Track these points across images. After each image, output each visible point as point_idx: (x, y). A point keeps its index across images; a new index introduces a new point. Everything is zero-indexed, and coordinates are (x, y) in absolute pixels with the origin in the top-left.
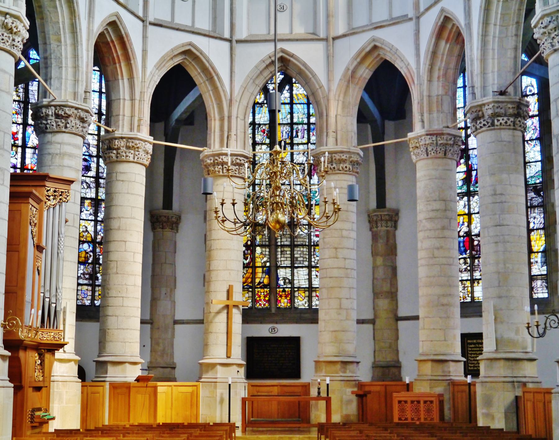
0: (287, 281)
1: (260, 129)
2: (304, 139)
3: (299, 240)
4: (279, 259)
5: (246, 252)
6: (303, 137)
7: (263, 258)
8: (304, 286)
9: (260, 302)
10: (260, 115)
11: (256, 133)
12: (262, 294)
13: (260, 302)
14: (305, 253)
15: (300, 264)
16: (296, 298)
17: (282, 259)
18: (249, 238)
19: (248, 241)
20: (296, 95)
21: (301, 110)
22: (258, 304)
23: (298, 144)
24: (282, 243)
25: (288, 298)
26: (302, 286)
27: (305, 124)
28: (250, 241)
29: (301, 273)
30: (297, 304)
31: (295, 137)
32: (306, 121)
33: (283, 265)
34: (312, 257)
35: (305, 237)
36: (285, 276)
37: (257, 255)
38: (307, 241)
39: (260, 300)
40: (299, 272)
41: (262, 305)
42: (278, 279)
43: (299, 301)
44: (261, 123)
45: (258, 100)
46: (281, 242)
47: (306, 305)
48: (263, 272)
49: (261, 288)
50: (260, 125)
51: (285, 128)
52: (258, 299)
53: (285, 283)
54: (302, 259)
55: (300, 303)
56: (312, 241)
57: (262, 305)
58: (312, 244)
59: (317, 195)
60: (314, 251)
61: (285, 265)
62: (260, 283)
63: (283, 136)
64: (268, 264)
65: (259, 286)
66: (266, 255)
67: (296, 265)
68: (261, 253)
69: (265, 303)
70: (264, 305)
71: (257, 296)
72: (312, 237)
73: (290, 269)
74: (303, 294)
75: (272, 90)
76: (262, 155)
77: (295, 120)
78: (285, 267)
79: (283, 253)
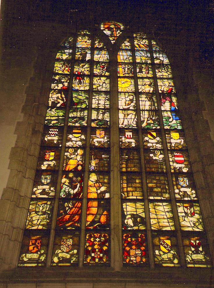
0: (138, 219)
1: (98, 65)
2: (149, 74)
3: (151, 166)
4: (125, 189)
5: (74, 179)
6: (148, 73)
7: (100, 187)
8: (168, 229)
9: (93, 255)
10: (99, 56)
11: (95, 67)
12: (98, 240)
13: (93, 255)
14: (163, 182)
15: (158, 196)
16: (156, 248)
17: (129, 189)
18: (80, 162)
19: (78, 165)
20: (137, 44)
21: (144, 55)
22: (90, 258)
23: (143, 78)
24: (129, 169)
25: (143, 248)
26: (164, 229)
27: (150, 64)
28: (81, 165)
29: (161, 208)
30: (160, 259)
31: (139, 72)
32: (149, 62)
33: (131, 198)
34: (175, 187)
35: (162, 163)
36: (135, 213)
37: (90, 183)
38: (164, 167)
39: (94, 251)
40: (157, 208)
41: (97, 260)
42: (124, 217)
43: (162, 253)
44: (100, 61)
45: (98, 46)
46: (127, 168)
47: (176, 261)
48: (99, 206)
49: (96, 230)
50: (98, 62)
51: (126, 66)
52: (90, 248)
53: (135, 223)
54: (159, 190)
55: (165, 257)
56: (172, 167)
57: (97, 260)
58: (172, 171)
59: (171, 120)
60: (177, 180)
61: (135, 198)
62: (93, 222)
63: (125, 71)
64: (107, 196)
65: (91, 228)
66: (105, 183)
67: (151, 198)
68: (97, 182)
69: (101, 255)
70: (101, 259)
71: (87, 244)
72: (171, 163)
73: (143, 204)
74: (168, 242)
75: (113, 40)
76: (101, 84)
77: (138, 60)
78: (135, 201)
79: (130, 181)
